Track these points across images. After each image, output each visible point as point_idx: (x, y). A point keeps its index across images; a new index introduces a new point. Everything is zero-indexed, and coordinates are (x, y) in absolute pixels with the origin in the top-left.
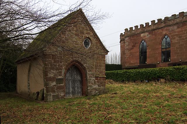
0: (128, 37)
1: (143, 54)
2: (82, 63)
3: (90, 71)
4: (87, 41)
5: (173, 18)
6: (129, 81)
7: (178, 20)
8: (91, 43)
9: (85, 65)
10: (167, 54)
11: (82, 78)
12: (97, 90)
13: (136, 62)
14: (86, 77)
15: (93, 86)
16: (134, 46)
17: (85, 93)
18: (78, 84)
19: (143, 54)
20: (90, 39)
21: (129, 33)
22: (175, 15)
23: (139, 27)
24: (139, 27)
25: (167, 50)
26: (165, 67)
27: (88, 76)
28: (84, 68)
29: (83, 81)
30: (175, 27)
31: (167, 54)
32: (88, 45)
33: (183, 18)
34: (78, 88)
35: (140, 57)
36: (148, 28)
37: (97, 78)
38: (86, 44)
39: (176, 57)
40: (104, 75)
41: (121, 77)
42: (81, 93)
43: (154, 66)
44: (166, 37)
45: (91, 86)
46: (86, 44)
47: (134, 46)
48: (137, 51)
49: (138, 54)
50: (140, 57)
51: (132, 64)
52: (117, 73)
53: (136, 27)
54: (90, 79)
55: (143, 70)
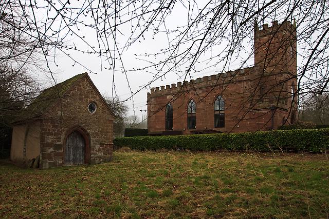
0: (154, 97)
1: (169, 117)
2: (86, 128)
3: (95, 137)
4: (93, 106)
5: (198, 81)
6: (149, 149)
7: (202, 84)
8: (97, 108)
9: (88, 131)
10: (192, 120)
11: (85, 144)
12: (101, 158)
13: (161, 127)
14: (90, 143)
15: (97, 152)
16: (160, 109)
17: (88, 162)
18: (80, 152)
19: (169, 117)
20: (96, 104)
21: (155, 94)
22: (200, 78)
23: (165, 88)
24: (165, 88)
25: (193, 115)
26: (187, 135)
27: (92, 143)
28: (88, 134)
29: (87, 148)
30: (200, 92)
31: (192, 120)
32: (94, 109)
33: (207, 82)
34: (80, 156)
35: (166, 121)
36: (174, 90)
37: (102, 145)
38: (92, 108)
39: (201, 124)
40: (111, 142)
41: (140, 144)
42: (84, 161)
43: (179, 133)
44: (192, 101)
45: (94, 154)
46: (92, 108)
47: (160, 109)
48: (163, 114)
49: (164, 118)
50: (167, 122)
51: (158, 129)
52: (137, 140)
53: (163, 87)
54: (95, 146)
55: (169, 137)
